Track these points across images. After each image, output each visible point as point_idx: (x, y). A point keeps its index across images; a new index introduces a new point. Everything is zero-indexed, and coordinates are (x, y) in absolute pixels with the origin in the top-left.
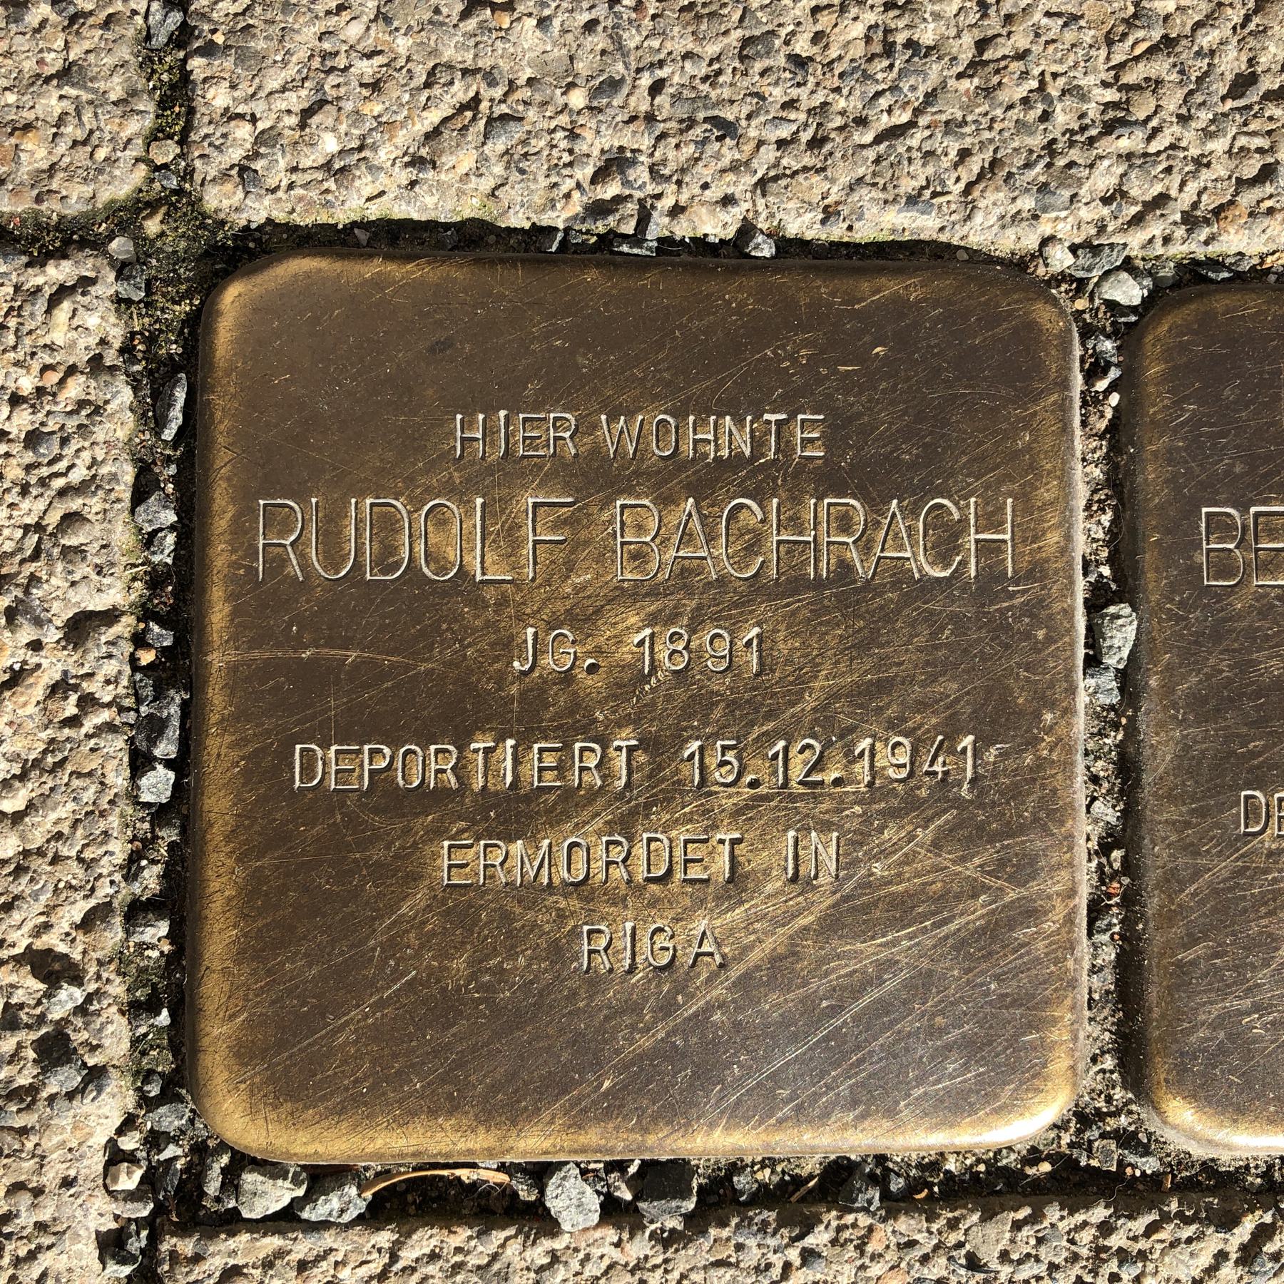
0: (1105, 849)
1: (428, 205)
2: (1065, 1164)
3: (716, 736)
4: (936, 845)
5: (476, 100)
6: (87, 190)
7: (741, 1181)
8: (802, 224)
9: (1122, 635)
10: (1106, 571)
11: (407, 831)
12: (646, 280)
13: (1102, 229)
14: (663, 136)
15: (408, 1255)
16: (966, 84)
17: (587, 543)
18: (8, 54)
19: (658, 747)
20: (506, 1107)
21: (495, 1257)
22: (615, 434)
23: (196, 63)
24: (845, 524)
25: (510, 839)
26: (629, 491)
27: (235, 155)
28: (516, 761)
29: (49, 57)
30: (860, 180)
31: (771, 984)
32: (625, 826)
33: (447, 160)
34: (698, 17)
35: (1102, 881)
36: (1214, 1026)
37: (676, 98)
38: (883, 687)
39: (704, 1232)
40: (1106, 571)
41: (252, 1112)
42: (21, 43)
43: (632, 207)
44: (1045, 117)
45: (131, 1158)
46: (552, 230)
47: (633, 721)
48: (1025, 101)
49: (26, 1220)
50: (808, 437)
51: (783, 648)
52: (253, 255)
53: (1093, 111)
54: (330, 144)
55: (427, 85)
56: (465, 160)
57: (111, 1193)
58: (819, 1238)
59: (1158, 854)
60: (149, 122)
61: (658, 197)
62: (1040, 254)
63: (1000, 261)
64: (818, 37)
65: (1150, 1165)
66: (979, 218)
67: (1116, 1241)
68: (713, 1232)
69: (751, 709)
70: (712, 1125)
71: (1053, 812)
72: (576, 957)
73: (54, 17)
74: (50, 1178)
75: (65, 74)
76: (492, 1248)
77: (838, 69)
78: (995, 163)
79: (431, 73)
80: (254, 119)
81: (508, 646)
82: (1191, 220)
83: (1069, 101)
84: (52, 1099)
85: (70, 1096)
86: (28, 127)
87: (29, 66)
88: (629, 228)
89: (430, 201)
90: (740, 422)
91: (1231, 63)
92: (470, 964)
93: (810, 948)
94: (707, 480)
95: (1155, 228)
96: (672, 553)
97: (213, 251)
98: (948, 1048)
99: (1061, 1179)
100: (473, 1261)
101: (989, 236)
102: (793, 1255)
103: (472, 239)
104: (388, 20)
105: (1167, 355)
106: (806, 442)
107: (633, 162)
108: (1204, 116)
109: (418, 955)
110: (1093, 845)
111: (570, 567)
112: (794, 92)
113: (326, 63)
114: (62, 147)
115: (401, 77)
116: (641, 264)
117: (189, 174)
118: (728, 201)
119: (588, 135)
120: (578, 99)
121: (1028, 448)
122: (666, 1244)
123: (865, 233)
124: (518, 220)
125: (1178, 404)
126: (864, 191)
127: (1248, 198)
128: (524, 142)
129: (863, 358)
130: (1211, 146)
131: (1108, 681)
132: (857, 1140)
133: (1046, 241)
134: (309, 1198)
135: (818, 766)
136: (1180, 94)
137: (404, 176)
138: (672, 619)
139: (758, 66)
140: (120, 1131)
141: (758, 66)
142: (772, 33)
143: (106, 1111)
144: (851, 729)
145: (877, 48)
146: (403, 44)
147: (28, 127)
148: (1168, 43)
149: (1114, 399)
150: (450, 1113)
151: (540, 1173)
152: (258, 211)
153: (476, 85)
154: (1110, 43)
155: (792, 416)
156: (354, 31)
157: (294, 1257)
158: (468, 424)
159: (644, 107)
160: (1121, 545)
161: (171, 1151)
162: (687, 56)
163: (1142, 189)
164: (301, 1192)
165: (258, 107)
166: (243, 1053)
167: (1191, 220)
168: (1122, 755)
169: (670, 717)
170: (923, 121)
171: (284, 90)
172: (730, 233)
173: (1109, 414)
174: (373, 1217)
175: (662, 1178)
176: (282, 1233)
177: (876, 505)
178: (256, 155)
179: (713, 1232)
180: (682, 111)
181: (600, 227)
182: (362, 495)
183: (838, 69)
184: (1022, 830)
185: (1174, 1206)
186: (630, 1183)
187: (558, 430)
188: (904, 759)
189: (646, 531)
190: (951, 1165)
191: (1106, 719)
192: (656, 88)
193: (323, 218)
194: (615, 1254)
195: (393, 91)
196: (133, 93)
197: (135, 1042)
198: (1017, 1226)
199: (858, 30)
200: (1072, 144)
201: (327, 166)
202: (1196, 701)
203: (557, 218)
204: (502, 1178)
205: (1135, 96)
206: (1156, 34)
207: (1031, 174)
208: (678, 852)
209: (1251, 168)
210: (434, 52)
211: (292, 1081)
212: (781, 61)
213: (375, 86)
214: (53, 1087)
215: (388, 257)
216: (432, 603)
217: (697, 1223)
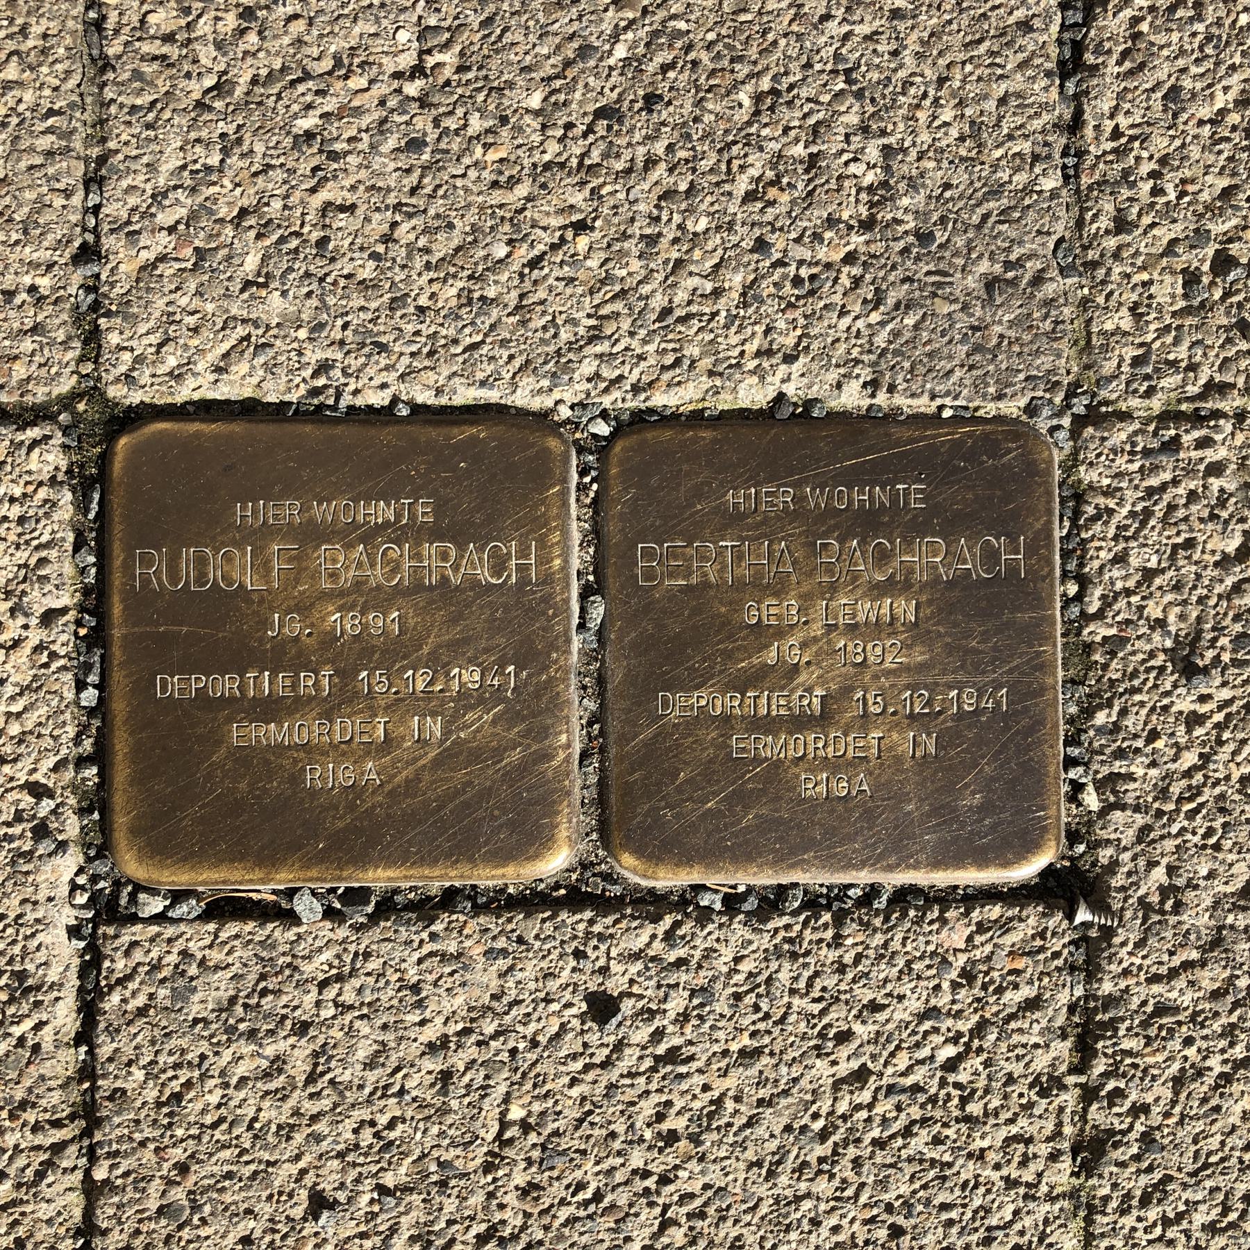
0: (590, 724)
1: (224, 392)
2: (573, 890)
3: (376, 668)
4: (494, 722)
5: (249, 335)
6: (47, 389)
7: (398, 898)
8: (424, 397)
9: (598, 612)
10: (591, 578)
11: (215, 719)
12: (339, 430)
13: (588, 395)
14: (348, 352)
15: (224, 935)
16: (512, 319)
17: (306, 569)
18: (5, 320)
19: (345, 675)
20: (268, 859)
21: (269, 937)
22: (322, 512)
23: (102, 321)
24: (444, 556)
25: (268, 723)
26: (328, 542)
27: (123, 369)
28: (270, 683)
29: (26, 321)
30: (454, 374)
31: (406, 795)
32: (328, 715)
33: (233, 368)
34: (367, 287)
35: (590, 740)
36: (646, 816)
37: (355, 332)
38: (466, 641)
39: (377, 924)
40: (591, 578)
41: (140, 861)
42: (12, 314)
43: (332, 391)
44: (555, 336)
45: (83, 888)
46: (291, 403)
47: (332, 662)
48: (544, 328)
49: (30, 917)
50: (424, 511)
51: (412, 622)
52: (133, 421)
53: (581, 331)
54: (172, 362)
55: (223, 329)
56: (243, 368)
57: (73, 906)
58: (438, 927)
59: (614, 726)
60: (78, 352)
61: (346, 385)
62: (553, 410)
63: (534, 414)
64: (433, 296)
65: (617, 890)
66: (519, 391)
67: (597, 928)
68: (382, 924)
69: (394, 653)
70: (377, 867)
71: (557, 705)
72: (304, 781)
73: (29, 299)
74: (41, 896)
75: (35, 329)
76: (267, 932)
77: (442, 313)
78: (528, 362)
79: (225, 322)
80: (132, 350)
81: (266, 623)
82: (636, 389)
83: (568, 327)
84: (40, 857)
85: (50, 855)
86: (16, 358)
87: (16, 325)
88: (331, 402)
89: (226, 390)
90: (388, 505)
91: (658, 302)
92: (249, 785)
93: (427, 777)
94: (370, 534)
95: (617, 394)
96: (352, 573)
97: (113, 419)
98: (501, 826)
99: (571, 896)
100: (257, 938)
101: (526, 401)
102: (425, 935)
103: (249, 409)
104: (202, 295)
105: (621, 463)
106: (424, 514)
107: (333, 367)
108: (643, 332)
109: (222, 781)
110: (584, 722)
111: (297, 581)
112: (419, 327)
113: (170, 319)
114: (34, 367)
115: (209, 325)
116: (336, 421)
117: (99, 379)
118: (384, 386)
119: (308, 353)
120: (303, 334)
121: (544, 514)
122: (358, 930)
123: (458, 401)
124: (272, 398)
125: (626, 490)
126: (456, 379)
127: (666, 377)
128: (274, 358)
129: (455, 469)
130: (647, 348)
131: (591, 637)
132: (456, 877)
133: (557, 403)
134: (172, 906)
135: (431, 683)
136: (629, 321)
137: (212, 377)
138: (352, 608)
139: (399, 313)
140: (76, 874)
141: (399, 313)
142: (407, 295)
143: (69, 863)
144: (448, 664)
145: (464, 301)
146: (210, 307)
147: (16, 358)
148: (623, 292)
149: (595, 487)
150: (240, 861)
151: (291, 893)
152: (136, 397)
153: (249, 329)
154: (591, 293)
155: (416, 500)
156: (184, 301)
157: (166, 936)
158: (243, 508)
159: (339, 336)
160: (598, 565)
161: (102, 884)
162: (362, 309)
163: (608, 373)
164: (167, 903)
165: (134, 343)
166: (134, 831)
167: (636, 389)
168: (600, 675)
169: (351, 657)
170: (489, 340)
171: (148, 333)
172: (386, 402)
173: (592, 495)
174: (205, 917)
175: (356, 896)
176: (159, 924)
177: (461, 548)
178: (133, 369)
179: (382, 924)
180: (359, 339)
181: (316, 402)
182: (188, 547)
183: (442, 313)
184: (540, 713)
185: (629, 911)
186: (340, 898)
187: (290, 510)
188: (477, 678)
189: (339, 563)
190: (511, 890)
191: (589, 656)
192: (345, 326)
193: (170, 400)
194: (331, 935)
195: (206, 333)
196: (70, 338)
197: (82, 828)
198: (544, 921)
199: (454, 291)
200: (570, 350)
201: (171, 374)
202: (634, 645)
203: (293, 397)
204: (274, 898)
205: (605, 323)
206: (617, 288)
207: (547, 368)
208: (357, 727)
209: (669, 359)
210: (227, 311)
211: (161, 843)
212: (412, 310)
213: (196, 330)
214: (40, 852)
215: (203, 421)
216: (228, 601)
217: (374, 919)
